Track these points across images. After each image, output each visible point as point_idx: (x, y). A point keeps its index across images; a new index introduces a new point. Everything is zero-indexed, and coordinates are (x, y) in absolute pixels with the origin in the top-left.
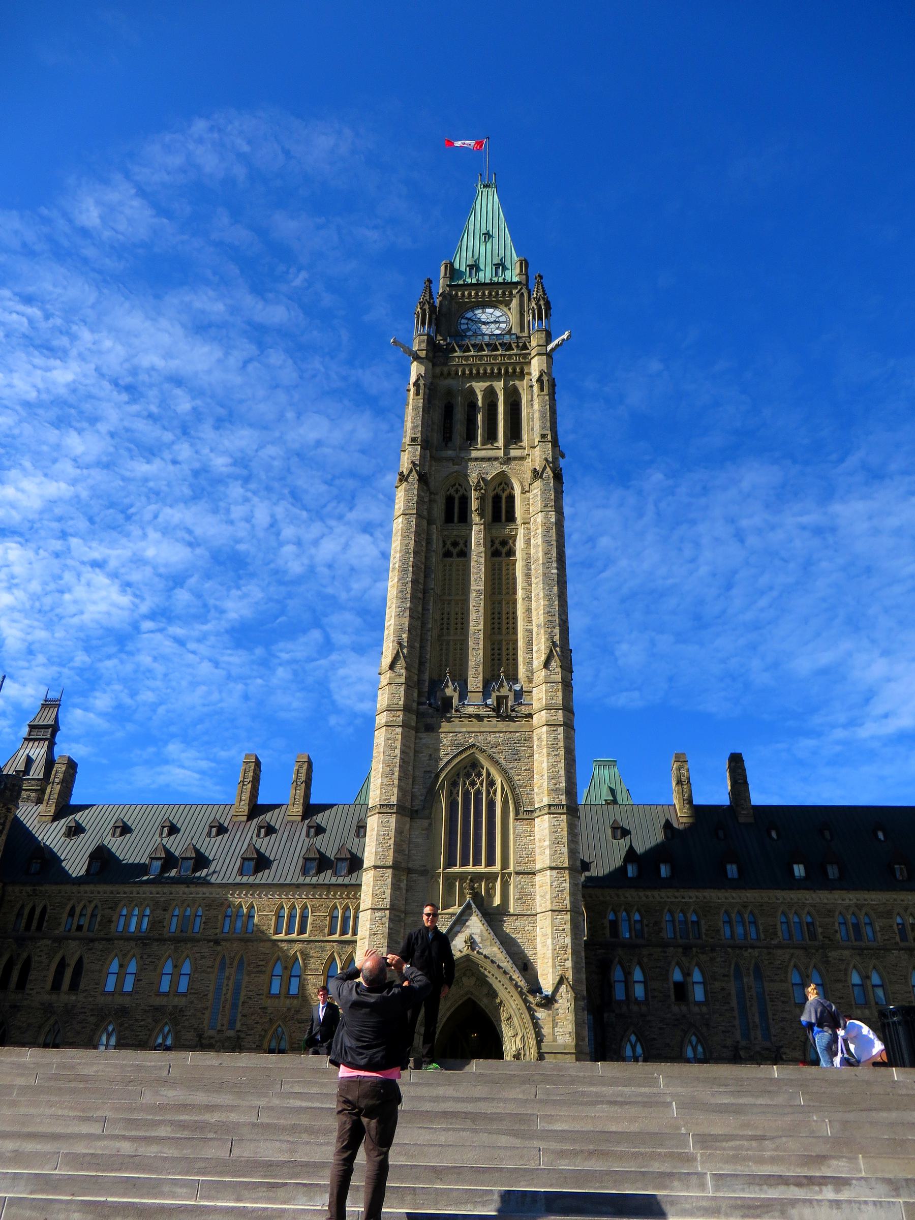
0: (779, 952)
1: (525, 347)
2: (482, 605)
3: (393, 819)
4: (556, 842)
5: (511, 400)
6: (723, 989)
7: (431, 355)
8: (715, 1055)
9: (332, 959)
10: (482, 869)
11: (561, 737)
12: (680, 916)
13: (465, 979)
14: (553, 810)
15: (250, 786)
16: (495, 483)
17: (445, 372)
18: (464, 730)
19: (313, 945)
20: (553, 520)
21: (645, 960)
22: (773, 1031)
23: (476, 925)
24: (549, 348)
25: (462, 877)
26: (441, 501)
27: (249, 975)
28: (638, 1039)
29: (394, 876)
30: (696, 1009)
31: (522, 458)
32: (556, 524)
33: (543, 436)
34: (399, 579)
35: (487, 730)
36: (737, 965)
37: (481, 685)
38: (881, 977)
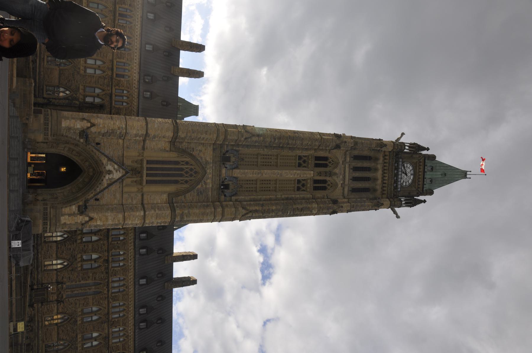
0: (106, 302)
6: (89, 277)
8: (59, 274)
12: (121, 258)
17: (386, 157)
21: (102, 242)
22: (70, 299)
23: (117, 175)
25: (142, 167)
28: (65, 238)
30: (79, 265)
34: (290, 136)
36: (101, 283)
37: (235, 175)
38: (96, 346)
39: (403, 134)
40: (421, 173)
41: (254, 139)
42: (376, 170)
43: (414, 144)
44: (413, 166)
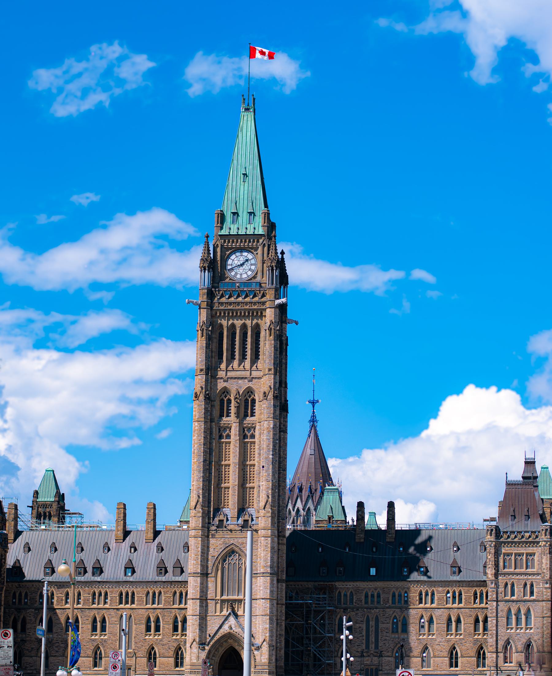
1: (263, 296)
2: (237, 471)
3: (199, 579)
4: (265, 588)
5: (255, 331)
7: (209, 303)
9: (176, 618)
10: (235, 597)
11: (270, 542)
13: (229, 640)
14: (264, 575)
15: (122, 522)
16: (246, 392)
18: (229, 536)
19: (166, 610)
20: (272, 426)
24: (278, 302)
25: (228, 601)
26: (217, 404)
27: (136, 624)
29: (200, 602)
31: (259, 378)
32: (273, 428)
33: (270, 370)
35: (239, 536)
37: (236, 514)
41: (201, 500)
42: (233, 325)
43: (201, 267)
44: (231, 254)
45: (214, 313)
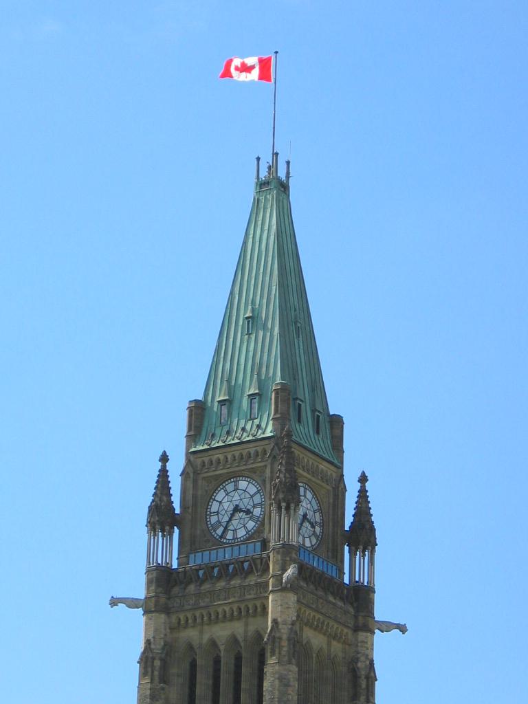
39: (114, 602)
40: (229, 457)
42: (213, 643)
44: (215, 490)
45: (174, 619)
